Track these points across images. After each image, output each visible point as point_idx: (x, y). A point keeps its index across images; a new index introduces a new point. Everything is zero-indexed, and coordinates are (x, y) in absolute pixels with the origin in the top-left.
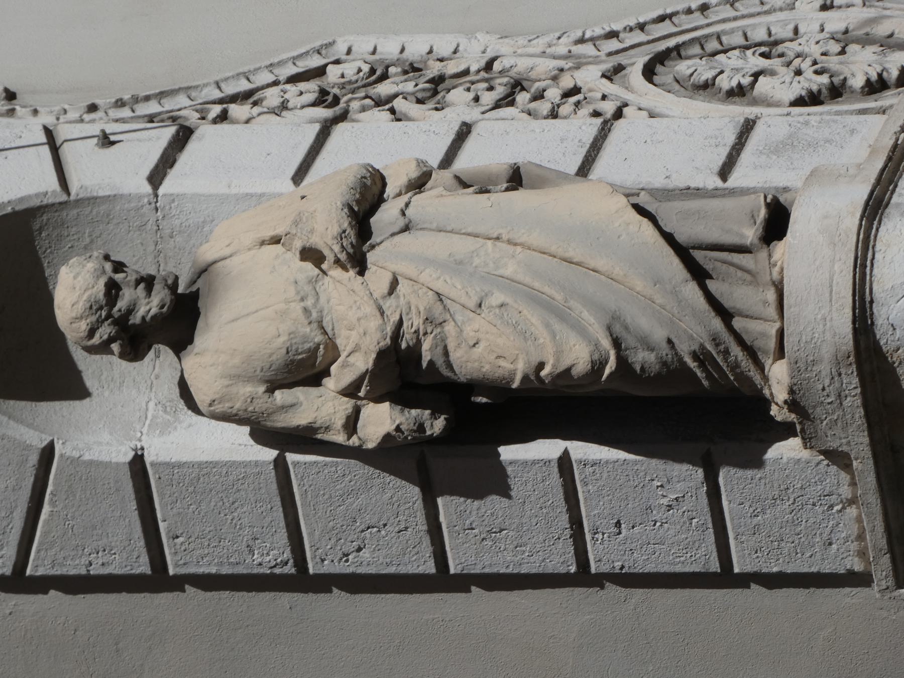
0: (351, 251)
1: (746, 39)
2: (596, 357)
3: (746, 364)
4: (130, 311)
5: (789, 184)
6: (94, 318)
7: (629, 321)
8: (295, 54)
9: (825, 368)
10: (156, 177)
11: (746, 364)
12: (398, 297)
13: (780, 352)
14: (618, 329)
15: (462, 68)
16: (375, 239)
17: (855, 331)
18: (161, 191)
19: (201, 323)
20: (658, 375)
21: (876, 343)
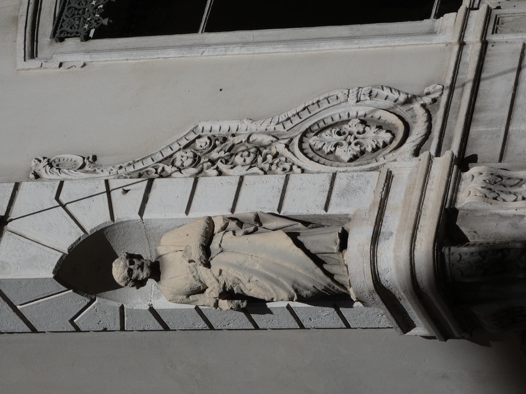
0: (204, 262)
1: (333, 120)
2: (290, 296)
3: (341, 289)
4: (138, 277)
5: (348, 213)
6: (126, 282)
7: (299, 282)
8: (185, 133)
9: (367, 293)
10: (141, 213)
11: (341, 289)
12: (223, 276)
13: (350, 286)
14: (296, 286)
15: (240, 141)
16: (212, 256)
17: (374, 285)
18: (144, 218)
19: (161, 276)
20: (312, 296)
21: (383, 286)
